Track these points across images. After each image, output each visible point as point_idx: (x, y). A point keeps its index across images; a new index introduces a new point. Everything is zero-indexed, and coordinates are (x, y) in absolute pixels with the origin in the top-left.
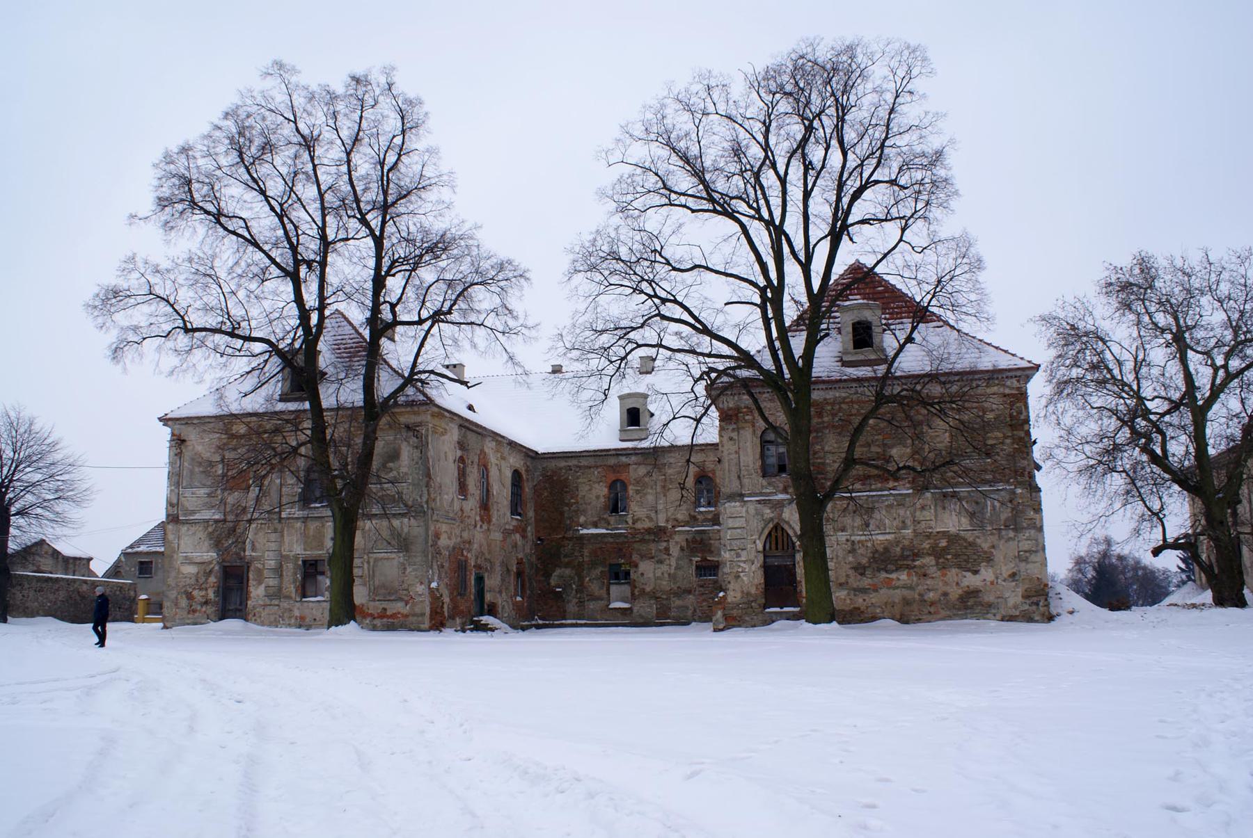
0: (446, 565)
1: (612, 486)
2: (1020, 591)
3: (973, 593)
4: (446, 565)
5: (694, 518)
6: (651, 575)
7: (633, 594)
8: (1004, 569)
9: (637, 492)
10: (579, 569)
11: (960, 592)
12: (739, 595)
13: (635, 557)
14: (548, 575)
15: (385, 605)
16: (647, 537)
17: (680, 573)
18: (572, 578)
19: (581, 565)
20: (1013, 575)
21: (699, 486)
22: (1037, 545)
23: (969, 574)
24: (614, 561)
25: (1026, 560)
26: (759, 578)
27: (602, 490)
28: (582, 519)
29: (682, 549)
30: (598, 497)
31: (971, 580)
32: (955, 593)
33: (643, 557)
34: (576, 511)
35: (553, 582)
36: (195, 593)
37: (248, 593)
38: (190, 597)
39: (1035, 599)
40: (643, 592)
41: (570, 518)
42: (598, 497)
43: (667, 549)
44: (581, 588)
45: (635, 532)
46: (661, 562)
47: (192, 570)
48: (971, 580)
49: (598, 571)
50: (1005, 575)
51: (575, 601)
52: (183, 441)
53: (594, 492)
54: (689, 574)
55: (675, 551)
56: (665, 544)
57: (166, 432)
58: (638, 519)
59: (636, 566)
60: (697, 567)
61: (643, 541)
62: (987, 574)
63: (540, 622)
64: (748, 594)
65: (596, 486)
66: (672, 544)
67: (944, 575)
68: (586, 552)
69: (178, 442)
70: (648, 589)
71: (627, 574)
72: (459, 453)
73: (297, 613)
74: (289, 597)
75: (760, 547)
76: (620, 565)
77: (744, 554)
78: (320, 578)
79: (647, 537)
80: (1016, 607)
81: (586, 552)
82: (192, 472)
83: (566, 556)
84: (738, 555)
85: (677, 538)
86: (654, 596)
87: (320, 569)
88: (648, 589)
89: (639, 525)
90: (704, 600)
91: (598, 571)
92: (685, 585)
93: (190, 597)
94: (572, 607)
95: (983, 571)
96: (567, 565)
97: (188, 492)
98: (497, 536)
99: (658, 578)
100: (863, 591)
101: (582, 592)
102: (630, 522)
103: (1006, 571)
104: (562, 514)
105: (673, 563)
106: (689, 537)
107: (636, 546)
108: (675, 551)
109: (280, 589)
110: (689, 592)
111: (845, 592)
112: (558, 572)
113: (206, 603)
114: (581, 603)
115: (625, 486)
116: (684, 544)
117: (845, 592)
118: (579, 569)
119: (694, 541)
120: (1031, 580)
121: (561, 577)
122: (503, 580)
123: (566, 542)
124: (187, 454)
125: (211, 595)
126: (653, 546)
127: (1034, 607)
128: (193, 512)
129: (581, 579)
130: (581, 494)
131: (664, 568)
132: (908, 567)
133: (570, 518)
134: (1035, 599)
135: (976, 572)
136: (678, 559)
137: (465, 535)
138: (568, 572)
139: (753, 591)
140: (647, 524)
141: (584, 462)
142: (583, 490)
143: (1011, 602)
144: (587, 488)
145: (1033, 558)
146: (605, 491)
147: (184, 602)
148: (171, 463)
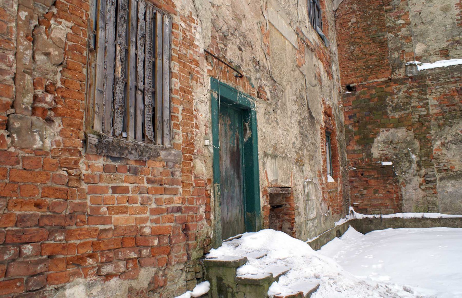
14: (366, 141)
18: (409, 144)
19: (423, 121)
28: (419, 49)
34: (407, 38)
35: (376, 152)
41: (397, 49)
44: (427, 159)
51: (417, 180)
63: (359, 216)
68: (432, 100)
81: (432, 100)
83: (395, 109)
94: (412, 190)
96: (398, 124)
101: (429, 165)
104: (383, 44)
112: (383, 135)
114: (428, 183)
122: (303, 136)
123: (394, 87)
129: (426, 143)
130: (413, 10)
133: (397, 49)
138: (401, 134)
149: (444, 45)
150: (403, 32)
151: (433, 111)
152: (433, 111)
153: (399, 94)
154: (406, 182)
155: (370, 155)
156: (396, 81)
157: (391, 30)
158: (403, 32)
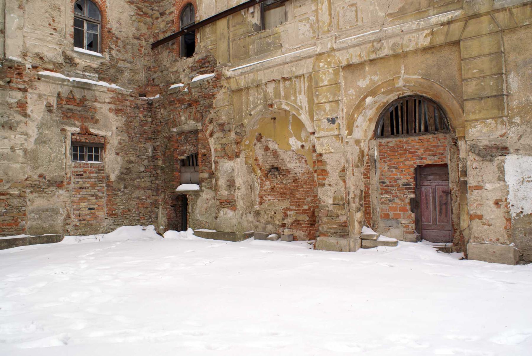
5: (70, 61)
17: (44, 150)
21: (79, 14)
43: (22, 106)
54: (58, 156)
55: (36, 110)
56: (19, 95)
66: (31, 97)
85: (42, 88)
90: (83, 199)
92: (52, 173)
105: (33, 130)
106: (64, 91)
108: (36, 110)
110: (59, 184)
116: (53, 101)
119: (71, 99)
136: (42, 126)
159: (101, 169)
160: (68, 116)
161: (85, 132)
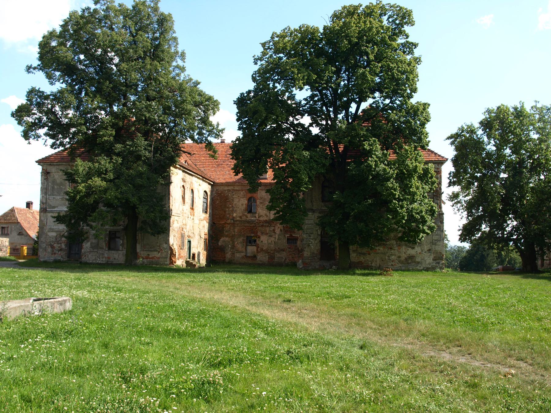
0: (177, 235)
1: (249, 200)
2: (432, 257)
3: (411, 257)
4: (177, 235)
6: (266, 242)
7: (257, 250)
8: (425, 247)
9: (261, 203)
10: (233, 237)
11: (406, 256)
12: (309, 254)
13: (259, 234)
14: (218, 240)
15: (149, 253)
16: (265, 224)
20: (429, 250)
22: (441, 238)
23: (410, 249)
24: (249, 235)
25: (435, 244)
26: (319, 247)
27: (244, 201)
29: (281, 230)
30: (242, 205)
31: (411, 252)
32: (404, 256)
33: (262, 233)
35: (220, 244)
36: (55, 245)
37: (82, 246)
38: (52, 247)
39: (438, 261)
40: (262, 250)
42: (242, 205)
43: (274, 230)
44: (233, 247)
45: (260, 221)
46: (271, 236)
47: (54, 234)
48: (411, 252)
49: (241, 240)
50: (426, 250)
51: (230, 253)
52: (48, 173)
53: (241, 202)
57: (39, 168)
58: (261, 216)
59: (259, 237)
60: (288, 239)
61: (262, 226)
62: (418, 249)
64: (313, 253)
65: (242, 199)
66: (276, 228)
67: (399, 249)
69: (45, 174)
70: (264, 249)
71: (255, 241)
72: (183, 184)
73: (106, 255)
74: (102, 248)
75: (319, 233)
76: (252, 237)
77: (312, 235)
78: (117, 240)
79: (265, 224)
80: (429, 264)
82: (53, 188)
83: (226, 232)
84: (310, 236)
86: (266, 251)
87: (118, 235)
88: (264, 249)
89: (261, 219)
90: (290, 255)
91: (241, 240)
93: (52, 247)
95: (416, 248)
96: (227, 236)
97: (51, 197)
98: (197, 221)
99: (270, 243)
100: (364, 254)
102: (257, 217)
103: (426, 248)
104: (225, 212)
107: (260, 228)
108: (278, 231)
109: (98, 245)
110: (283, 250)
111: (355, 254)
113: (61, 250)
115: (255, 201)
116: (282, 228)
117: (355, 254)
118: (233, 237)
120: (437, 253)
121: (223, 241)
124: (50, 179)
125: (63, 246)
126: (268, 229)
127: (437, 265)
128: (54, 207)
129: (233, 242)
130: (235, 203)
131: (273, 239)
132: (384, 244)
134: (438, 261)
135: (413, 248)
136: (279, 235)
137: (184, 222)
138: (227, 239)
139: (316, 252)
140: (265, 218)
141: (236, 188)
142: (236, 201)
143: (427, 262)
144: (237, 200)
145: (438, 243)
146: (246, 202)
147: (49, 250)
148: (42, 183)
149: (241, 215)
150: (231, 209)
151: (236, 233)
152: (236, 233)
153: (228, 227)
154: (227, 253)
155: (218, 245)
156: (227, 224)
157: (228, 208)
158: (231, 209)
159: (296, 246)
160: (286, 232)
161: (291, 236)
